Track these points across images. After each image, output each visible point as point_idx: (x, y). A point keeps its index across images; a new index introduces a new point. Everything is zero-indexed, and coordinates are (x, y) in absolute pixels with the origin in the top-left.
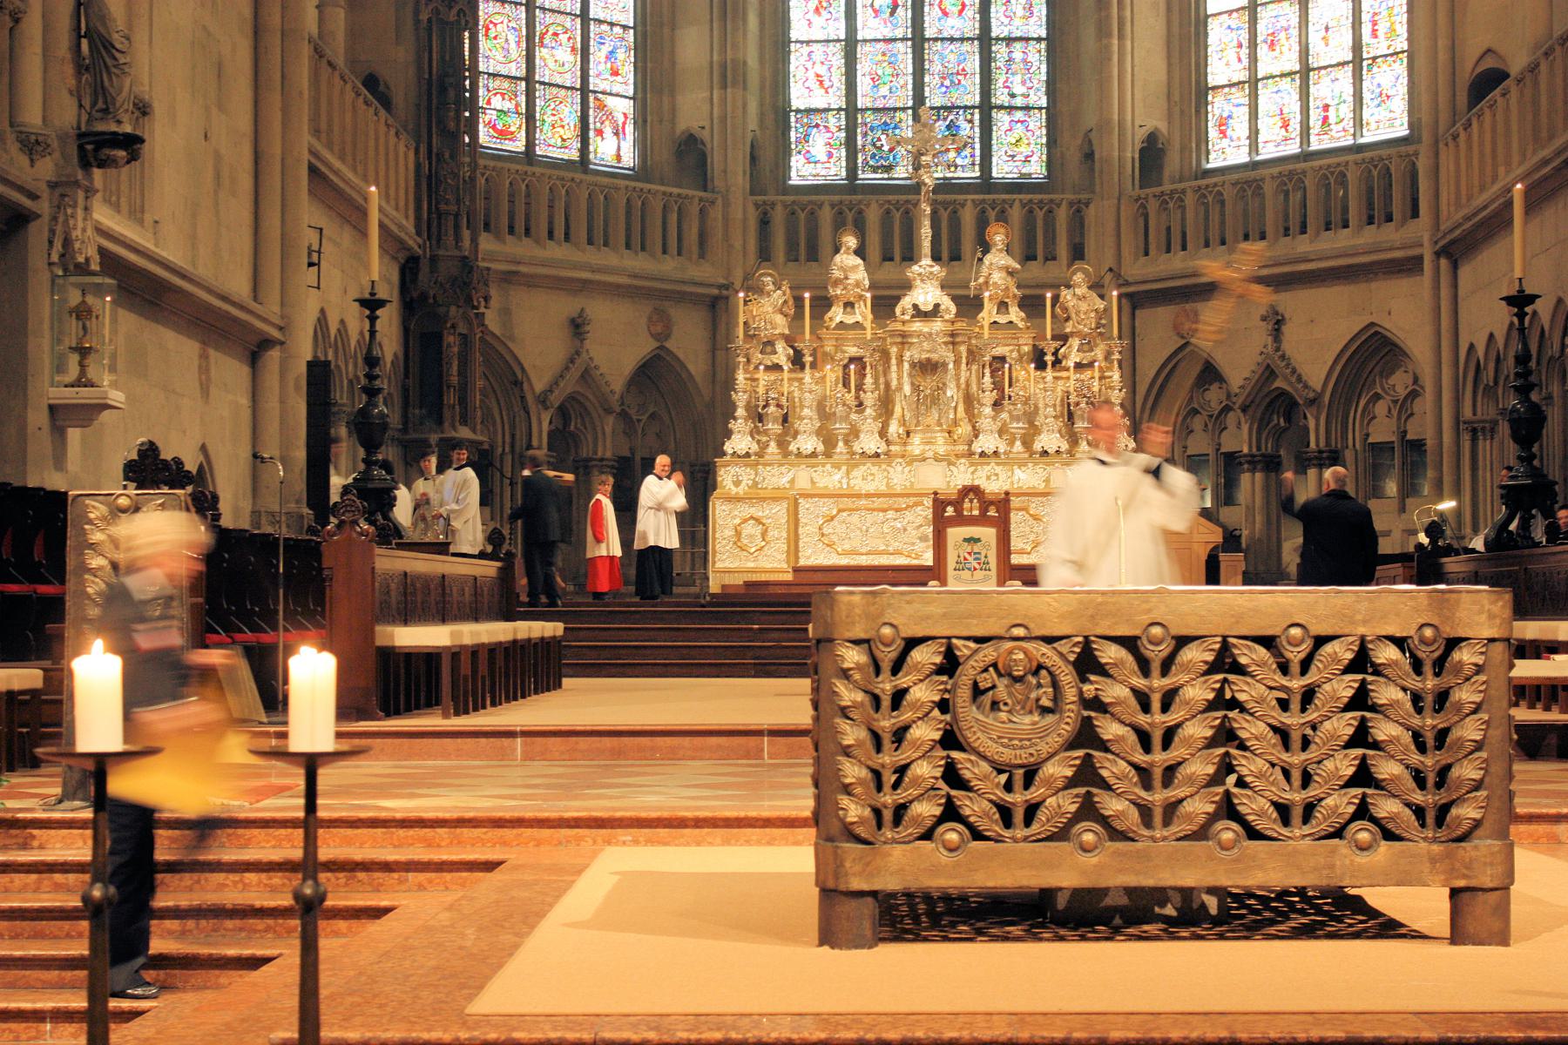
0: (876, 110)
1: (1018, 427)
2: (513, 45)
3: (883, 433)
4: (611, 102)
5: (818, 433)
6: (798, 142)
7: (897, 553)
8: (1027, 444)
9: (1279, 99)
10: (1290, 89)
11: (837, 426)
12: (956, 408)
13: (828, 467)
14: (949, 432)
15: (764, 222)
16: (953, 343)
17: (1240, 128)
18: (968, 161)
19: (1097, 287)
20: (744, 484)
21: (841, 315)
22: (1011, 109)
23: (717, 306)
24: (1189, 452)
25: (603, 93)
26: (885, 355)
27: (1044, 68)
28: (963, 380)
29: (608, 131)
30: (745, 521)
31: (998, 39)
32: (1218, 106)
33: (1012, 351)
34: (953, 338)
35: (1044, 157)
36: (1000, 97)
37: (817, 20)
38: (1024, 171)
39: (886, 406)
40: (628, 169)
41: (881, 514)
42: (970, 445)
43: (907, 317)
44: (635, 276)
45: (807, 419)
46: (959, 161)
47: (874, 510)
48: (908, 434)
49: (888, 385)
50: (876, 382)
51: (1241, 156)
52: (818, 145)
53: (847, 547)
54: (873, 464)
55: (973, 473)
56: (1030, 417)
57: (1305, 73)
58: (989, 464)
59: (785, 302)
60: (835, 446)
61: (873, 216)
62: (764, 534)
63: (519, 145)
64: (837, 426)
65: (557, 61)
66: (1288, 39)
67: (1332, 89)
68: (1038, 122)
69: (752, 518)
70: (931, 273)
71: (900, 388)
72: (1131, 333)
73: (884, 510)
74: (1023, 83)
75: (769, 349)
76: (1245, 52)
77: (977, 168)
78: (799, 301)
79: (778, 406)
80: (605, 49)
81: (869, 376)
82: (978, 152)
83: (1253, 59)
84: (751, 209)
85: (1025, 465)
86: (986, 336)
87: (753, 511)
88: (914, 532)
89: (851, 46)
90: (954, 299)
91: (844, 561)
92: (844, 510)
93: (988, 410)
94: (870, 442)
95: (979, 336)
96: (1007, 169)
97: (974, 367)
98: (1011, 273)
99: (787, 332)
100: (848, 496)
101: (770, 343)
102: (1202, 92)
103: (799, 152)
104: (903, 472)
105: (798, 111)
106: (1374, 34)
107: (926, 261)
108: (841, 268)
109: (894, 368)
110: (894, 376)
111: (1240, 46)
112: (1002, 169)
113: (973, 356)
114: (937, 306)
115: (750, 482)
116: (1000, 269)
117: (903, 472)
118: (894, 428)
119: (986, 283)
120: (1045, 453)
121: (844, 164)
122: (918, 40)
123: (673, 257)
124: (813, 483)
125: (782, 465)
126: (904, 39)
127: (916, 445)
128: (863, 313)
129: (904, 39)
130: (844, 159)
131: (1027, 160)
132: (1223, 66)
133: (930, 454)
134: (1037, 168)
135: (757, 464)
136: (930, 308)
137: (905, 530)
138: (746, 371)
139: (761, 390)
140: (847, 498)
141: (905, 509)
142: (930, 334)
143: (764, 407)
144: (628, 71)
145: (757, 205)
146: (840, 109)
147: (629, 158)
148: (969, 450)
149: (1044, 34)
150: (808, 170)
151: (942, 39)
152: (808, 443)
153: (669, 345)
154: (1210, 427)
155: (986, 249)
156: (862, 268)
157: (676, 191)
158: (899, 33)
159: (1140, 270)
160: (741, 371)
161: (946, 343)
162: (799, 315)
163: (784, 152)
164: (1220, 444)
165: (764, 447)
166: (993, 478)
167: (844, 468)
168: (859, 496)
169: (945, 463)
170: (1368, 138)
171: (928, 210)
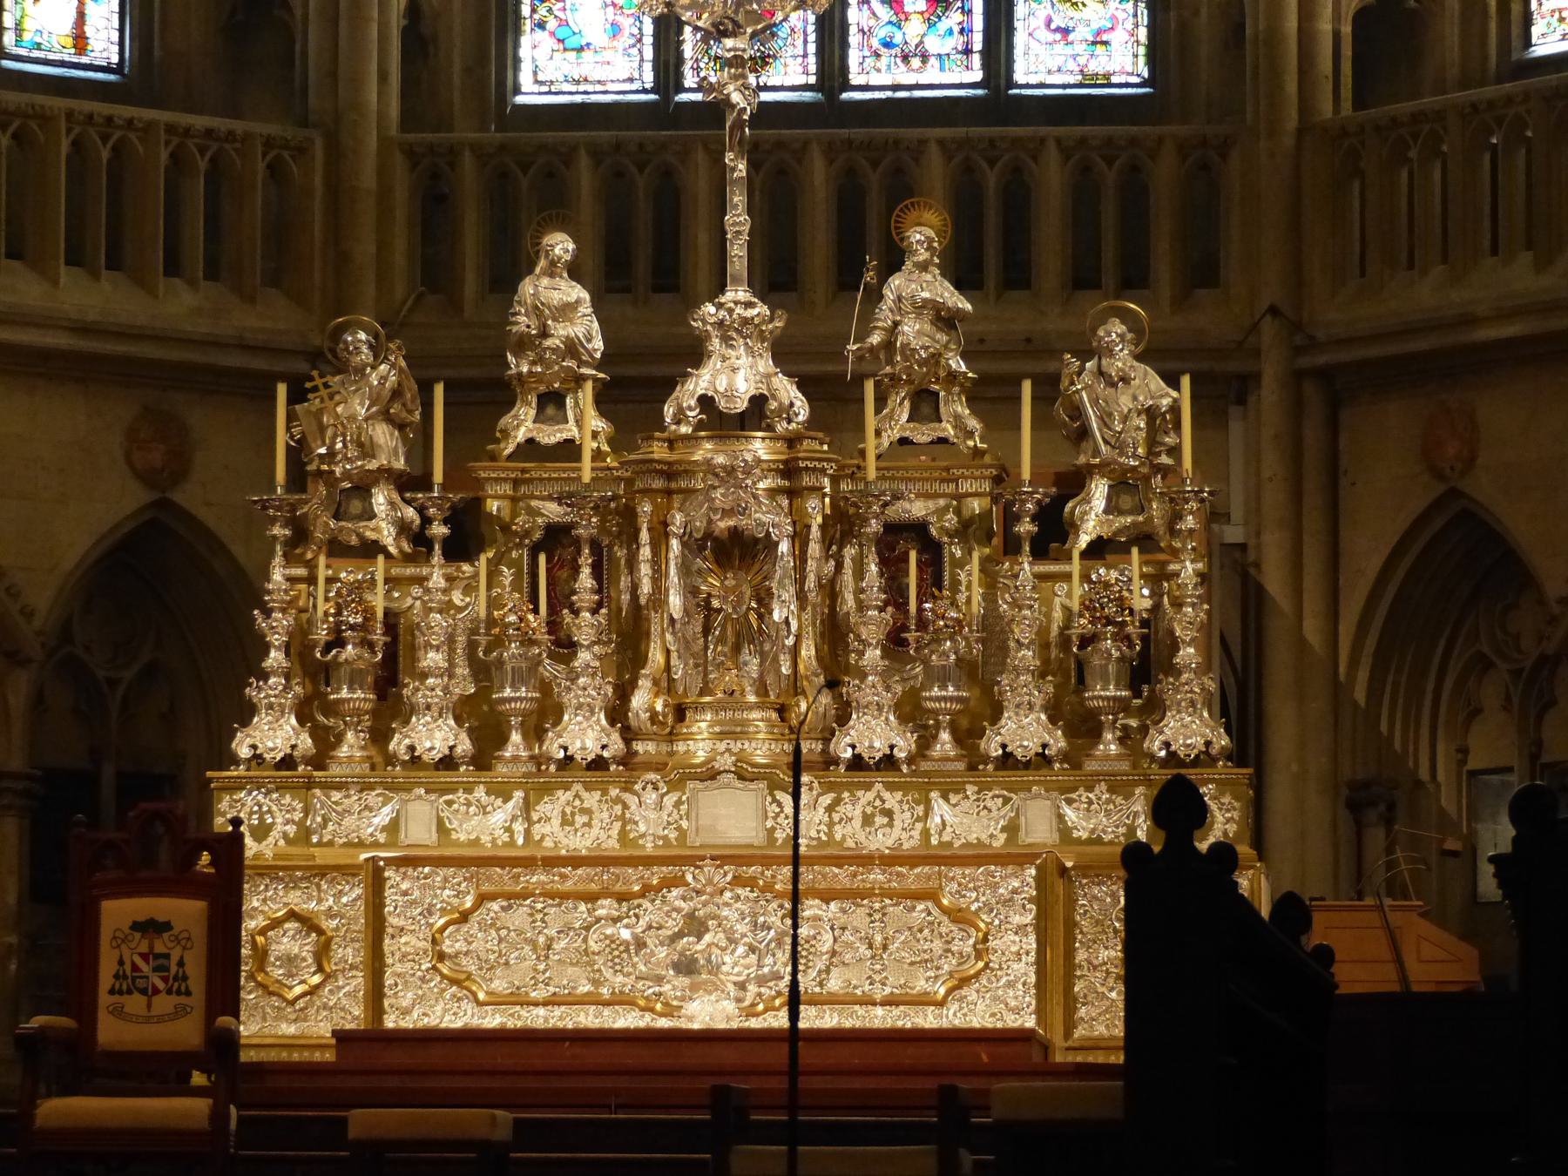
3: (617, 713)
5: (463, 711)
7: (621, 1000)
8: (968, 737)
11: (508, 692)
12: (795, 652)
13: (480, 793)
14: (782, 710)
16: (792, 493)
18: (957, 41)
20: (275, 833)
21: (529, 424)
24: (1472, 765)
28: (811, 582)
30: (276, 923)
33: (941, 512)
35: (1143, 34)
38: (1095, 66)
40: (105, 69)
41: (583, 907)
42: (827, 741)
43: (685, 429)
44: (83, 329)
46: (933, 45)
47: (564, 896)
48: (680, 713)
53: (499, 985)
54: (589, 787)
55: (830, 809)
58: (868, 787)
59: (397, 393)
60: (503, 740)
62: (322, 954)
64: (508, 692)
69: (292, 915)
70: (746, 321)
73: (591, 898)
75: (356, 506)
77: (976, 60)
81: (586, 572)
82: (978, 22)
84: (399, 161)
85: (959, 789)
86: (872, 474)
87: (295, 899)
88: (662, 953)
90: (805, 385)
91: (492, 1020)
92: (493, 897)
93: (873, 655)
95: (857, 473)
96: (1059, 61)
97: (850, 552)
98: (945, 319)
99: (400, 464)
100: (528, 863)
101: (362, 488)
103: (541, 25)
104: (660, 806)
107: (737, 294)
108: (536, 311)
109: (645, 552)
110: (645, 570)
113: (842, 526)
114: (758, 402)
115: (291, 830)
116: (921, 307)
117: (660, 806)
118: (639, 700)
119: (889, 345)
120: (1007, 760)
121: (649, 53)
123: (192, 283)
125: (366, 787)
130: (648, 40)
133: (726, 762)
135: (310, 784)
136: (741, 405)
137: (640, 944)
138: (289, 559)
141: (642, 894)
142: (730, 470)
143: (328, 647)
145: (411, 153)
148: (825, 751)
153: (187, 497)
154: (1516, 700)
155: (894, 260)
156: (586, 309)
157: (199, 122)
160: (278, 560)
161: (772, 493)
164: (1539, 744)
165: (326, 743)
166: (880, 820)
167: (518, 795)
168: (551, 862)
169: (762, 785)
171: (741, 169)
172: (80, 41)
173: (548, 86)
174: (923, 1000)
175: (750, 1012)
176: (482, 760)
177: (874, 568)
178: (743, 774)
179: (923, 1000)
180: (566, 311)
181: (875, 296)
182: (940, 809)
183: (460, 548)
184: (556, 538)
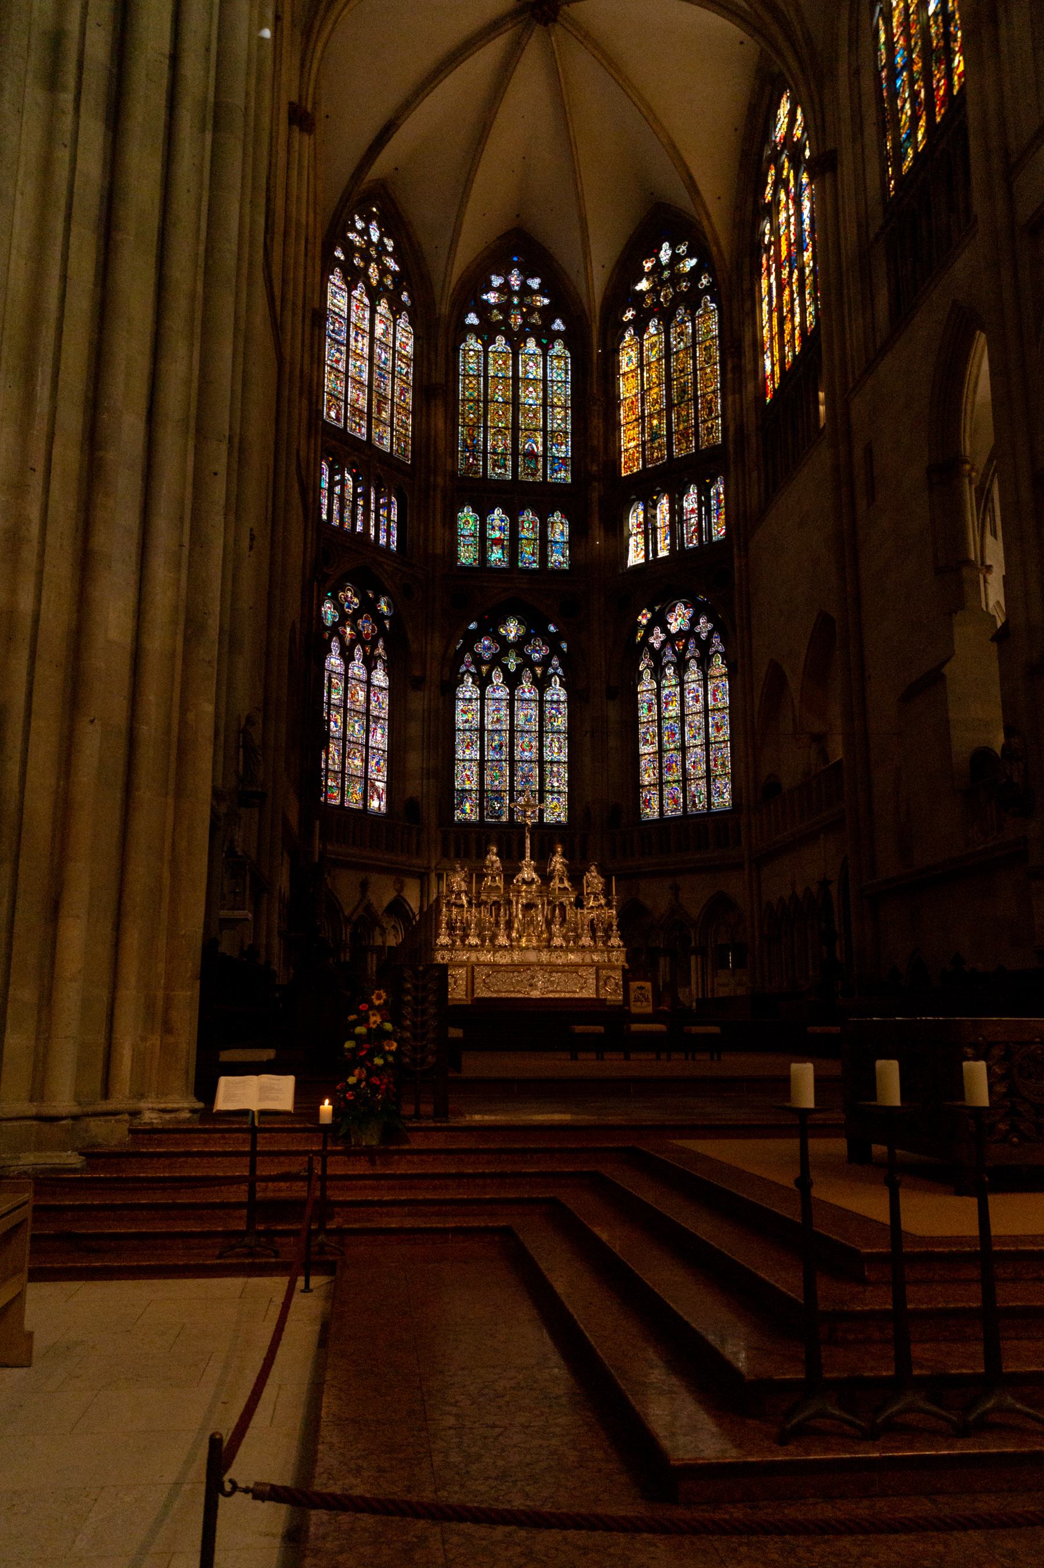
0: (492, 791)
2: (336, 757)
3: (509, 937)
4: (377, 784)
5: (478, 936)
6: (457, 804)
7: (519, 992)
17: (655, 804)
19: (603, 872)
22: (552, 793)
25: (374, 779)
26: (509, 902)
27: (566, 775)
29: (375, 796)
31: (546, 761)
32: (644, 794)
34: (541, 893)
36: (548, 788)
37: (467, 752)
39: (509, 925)
48: (520, 937)
49: (511, 914)
50: (505, 914)
51: (656, 816)
52: (467, 807)
56: (575, 930)
57: (685, 780)
63: (338, 802)
65: (355, 763)
66: (676, 766)
67: (697, 788)
68: (563, 799)
71: (517, 916)
74: (558, 781)
76: (656, 771)
78: (471, 875)
79: (462, 923)
80: (374, 761)
83: (661, 774)
89: (482, 763)
90: (540, 876)
91: (495, 995)
94: (502, 940)
101: (458, 894)
102: (637, 786)
105: (458, 790)
106: (716, 765)
111: (654, 768)
112: (548, 818)
118: (514, 935)
122: (512, 762)
124: (478, 958)
126: (505, 760)
127: (524, 943)
128: (499, 882)
129: (505, 760)
131: (559, 815)
132: (647, 778)
139: (454, 916)
144: (384, 770)
146: (476, 790)
147: (383, 809)
149: (566, 760)
150: (461, 816)
151: (523, 761)
155: (554, 853)
158: (503, 757)
162: (471, 882)
165: (454, 942)
170: (714, 809)
172: (379, 808)
173: (460, 820)
174: (575, 992)
175: (543, 994)
176: (483, 945)
177: (557, 911)
178: (534, 948)
179: (575, 992)
180: (496, 861)
181: (551, 860)
182: (572, 957)
183: (479, 905)
184: (495, 903)
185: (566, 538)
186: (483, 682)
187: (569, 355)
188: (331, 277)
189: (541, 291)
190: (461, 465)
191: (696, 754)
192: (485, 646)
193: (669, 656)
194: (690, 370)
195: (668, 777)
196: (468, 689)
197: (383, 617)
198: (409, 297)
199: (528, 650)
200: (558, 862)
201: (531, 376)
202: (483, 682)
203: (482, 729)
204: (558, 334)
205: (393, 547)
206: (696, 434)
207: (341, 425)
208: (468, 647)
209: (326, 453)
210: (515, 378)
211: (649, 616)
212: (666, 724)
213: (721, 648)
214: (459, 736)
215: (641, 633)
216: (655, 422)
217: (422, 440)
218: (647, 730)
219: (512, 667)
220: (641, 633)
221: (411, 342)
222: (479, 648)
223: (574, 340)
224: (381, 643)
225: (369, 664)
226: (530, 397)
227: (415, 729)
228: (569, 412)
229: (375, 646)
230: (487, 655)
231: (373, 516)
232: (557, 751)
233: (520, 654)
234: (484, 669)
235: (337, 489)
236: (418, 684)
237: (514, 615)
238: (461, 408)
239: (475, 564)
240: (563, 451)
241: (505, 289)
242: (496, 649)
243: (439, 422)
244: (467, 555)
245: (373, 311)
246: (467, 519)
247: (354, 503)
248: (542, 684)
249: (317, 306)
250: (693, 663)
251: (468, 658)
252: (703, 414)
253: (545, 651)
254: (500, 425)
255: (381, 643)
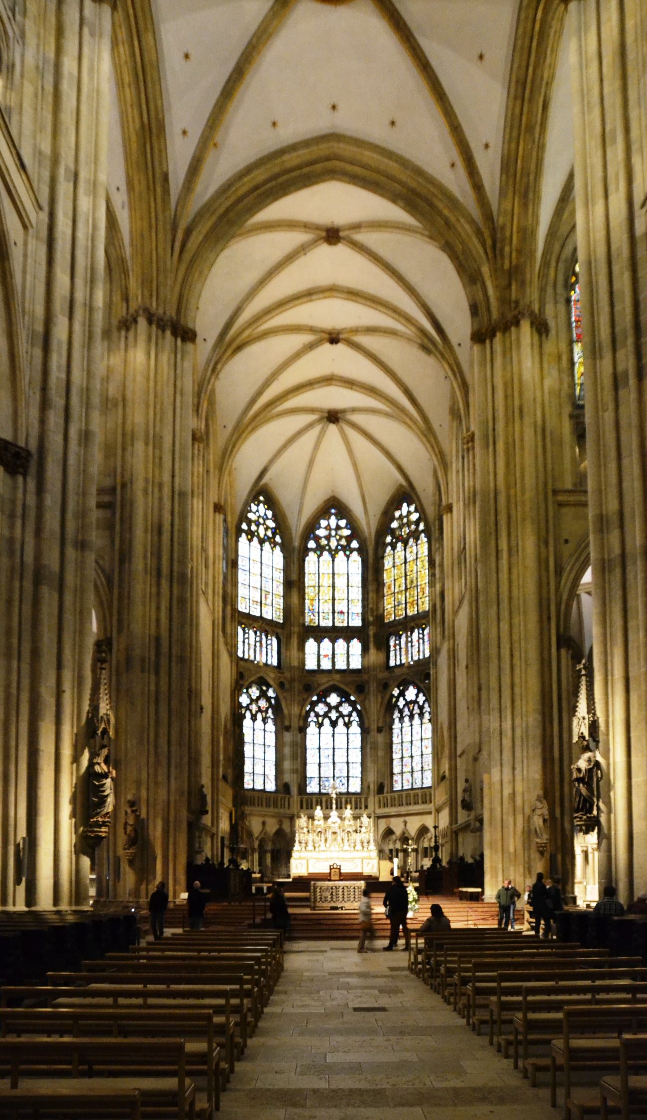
1: (353, 845)
9: (407, 776)
10: (409, 775)
15: (302, 802)
23: (292, 819)
32: (395, 778)
39: (326, 840)
45: (310, 844)
51: (400, 788)
61: (324, 800)
68: (359, 780)
72: (376, 826)
94: (323, 847)
101: (302, 828)
102: (392, 774)
112: (351, 790)
118: (328, 845)
122: (334, 763)
127: (332, 848)
128: (322, 822)
132: (396, 769)
134: (359, 790)
140: (318, 859)
152: (310, 847)
159: (380, 811)
163: (306, 786)
184: (320, 832)
185: (360, 652)
186: (320, 725)
187: (359, 559)
188: (240, 539)
189: (346, 527)
190: (307, 620)
191: (417, 759)
192: (321, 709)
193: (406, 712)
194: (415, 571)
195: (404, 770)
196: (312, 730)
197: (271, 698)
198: (281, 538)
199: (341, 709)
200: (348, 812)
201: (341, 572)
202: (320, 725)
203: (319, 749)
204: (354, 549)
205: (275, 663)
206: (417, 604)
207: (247, 611)
208: (312, 709)
209: (240, 624)
210: (333, 574)
211: (398, 691)
212: (404, 745)
213: (429, 710)
214: (308, 751)
215: (394, 700)
216: (400, 596)
217: (287, 611)
218: (396, 748)
219: (334, 718)
220: (394, 700)
221: (282, 559)
222: (317, 709)
223: (361, 551)
224: (270, 711)
225: (264, 720)
226: (341, 582)
227: (287, 750)
228: (360, 589)
229: (266, 712)
230: (321, 713)
231: (264, 650)
232: (356, 756)
233: (338, 711)
234: (320, 719)
235: (246, 641)
236: (288, 729)
237: (334, 691)
238: (306, 591)
239: (316, 668)
240: (357, 608)
241: (328, 528)
242: (326, 709)
243: (295, 600)
244: (311, 664)
245: (262, 550)
246: (311, 645)
247: (255, 646)
248: (347, 725)
249: (233, 557)
250: (416, 717)
251: (312, 714)
252: (420, 595)
253: (350, 709)
254: (327, 598)
255: (270, 711)
